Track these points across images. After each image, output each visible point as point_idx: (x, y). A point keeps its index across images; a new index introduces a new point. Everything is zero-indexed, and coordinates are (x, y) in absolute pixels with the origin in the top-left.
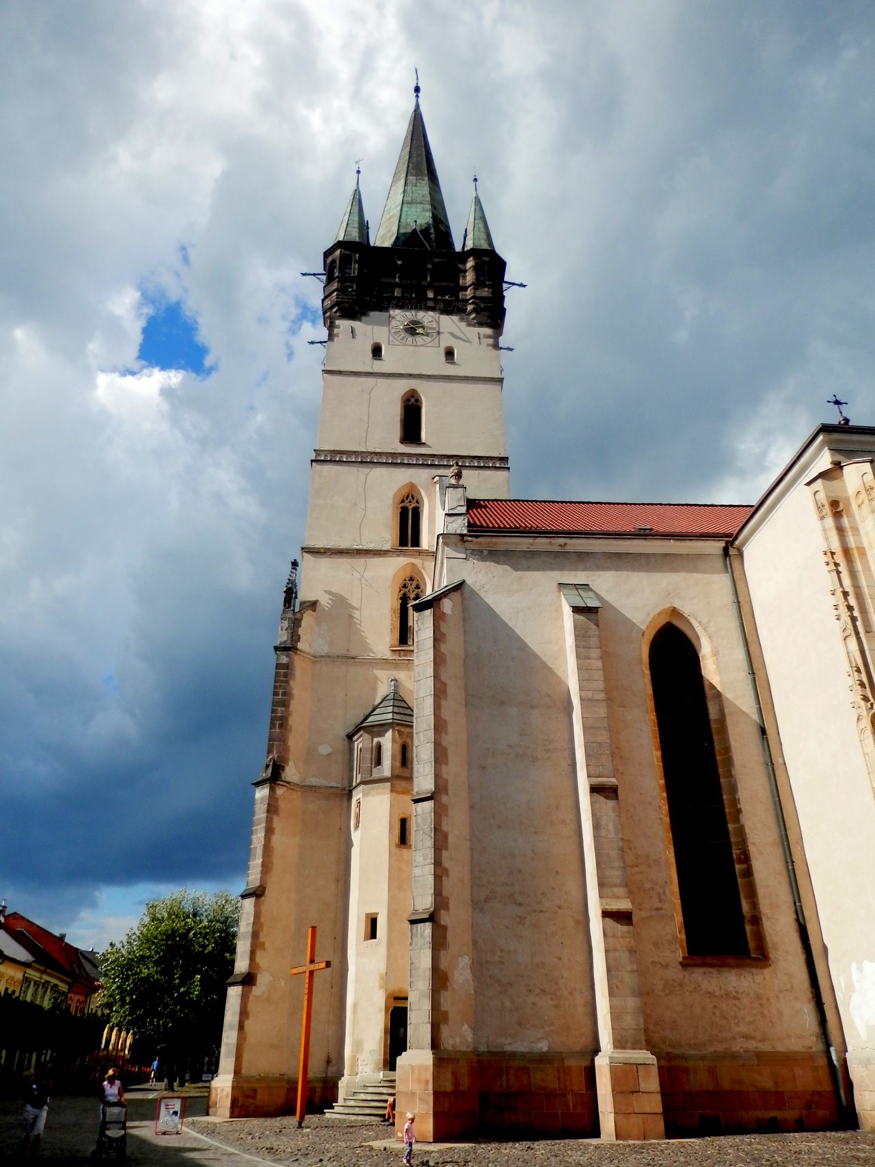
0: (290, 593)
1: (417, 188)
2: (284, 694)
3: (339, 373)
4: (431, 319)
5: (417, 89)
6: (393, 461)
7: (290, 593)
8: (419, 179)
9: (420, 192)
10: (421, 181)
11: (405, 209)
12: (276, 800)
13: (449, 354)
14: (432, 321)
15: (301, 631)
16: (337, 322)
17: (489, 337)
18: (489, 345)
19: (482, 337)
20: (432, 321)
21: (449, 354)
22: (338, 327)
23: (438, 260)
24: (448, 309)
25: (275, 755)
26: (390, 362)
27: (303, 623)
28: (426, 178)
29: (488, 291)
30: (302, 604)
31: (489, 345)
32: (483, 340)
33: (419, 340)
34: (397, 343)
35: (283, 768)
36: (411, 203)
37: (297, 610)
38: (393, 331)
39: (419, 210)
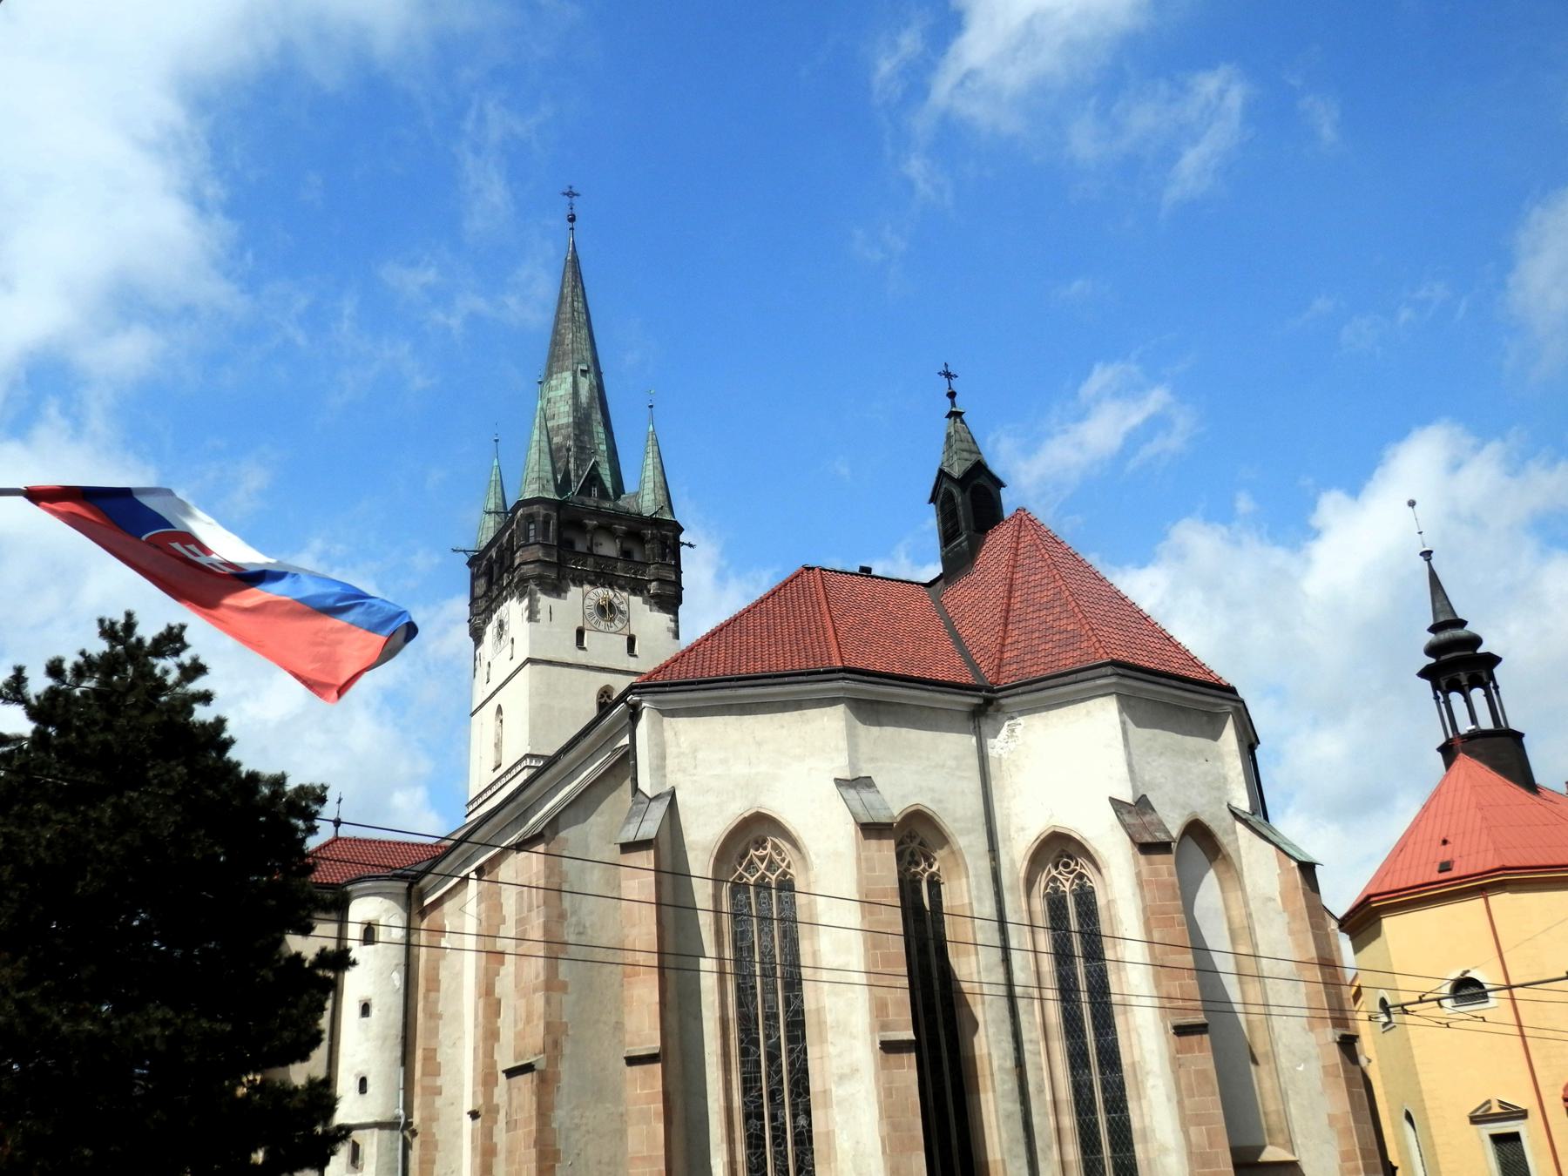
5: (572, 219)
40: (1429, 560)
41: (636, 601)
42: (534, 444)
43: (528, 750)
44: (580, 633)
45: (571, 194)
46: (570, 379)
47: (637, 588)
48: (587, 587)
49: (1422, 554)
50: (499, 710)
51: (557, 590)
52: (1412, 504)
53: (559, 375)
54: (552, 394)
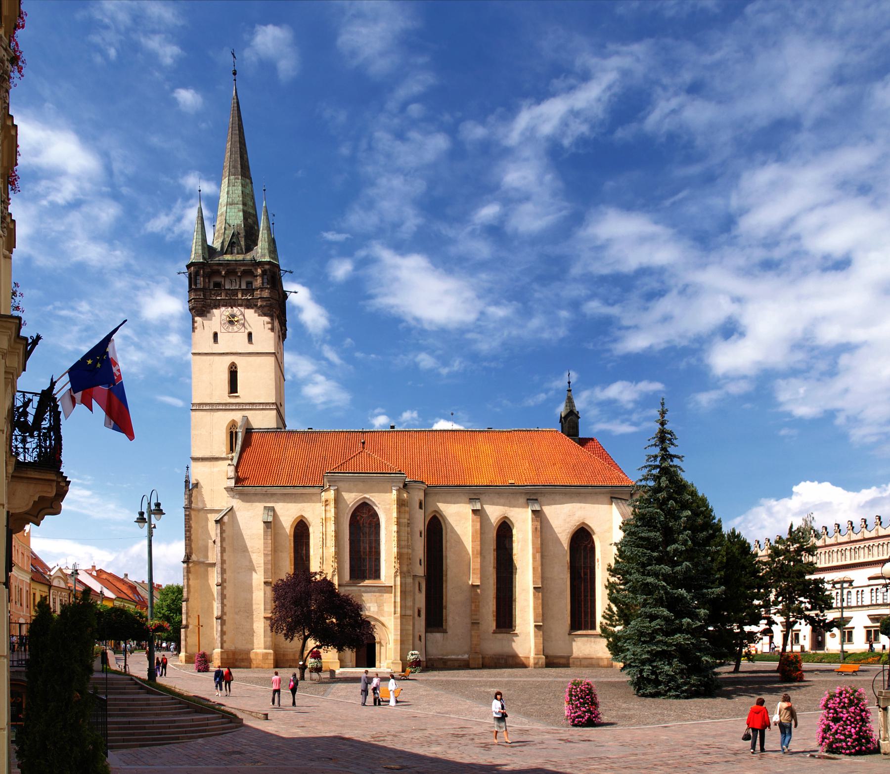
0: (187, 482)
1: (235, 188)
2: (189, 527)
3: (199, 354)
7: (187, 482)
9: (236, 192)
11: (228, 210)
17: (268, 323)
18: (269, 329)
19: (265, 323)
24: (249, 305)
28: (240, 177)
30: (193, 484)
31: (269, 329)
32: (266, 325)
33: (235, 327)
35: (191, 556)
37: (190, 488)
38: (223, 322)
39: (236, 211)
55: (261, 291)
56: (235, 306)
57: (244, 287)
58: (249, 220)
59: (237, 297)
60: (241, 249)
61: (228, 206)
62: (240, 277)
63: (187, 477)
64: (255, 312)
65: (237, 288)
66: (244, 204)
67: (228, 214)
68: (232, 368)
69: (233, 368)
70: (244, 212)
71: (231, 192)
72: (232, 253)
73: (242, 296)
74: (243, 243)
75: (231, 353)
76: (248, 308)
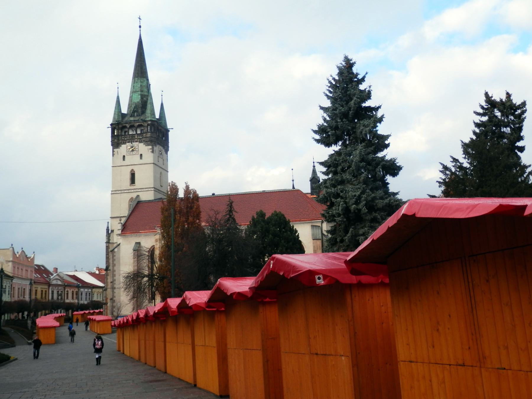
0: (108, 230)
1: (137, 84)
2: (108, 252)
4: (136, 145)
5: (140, 27)
6: (128, 191)
8: (138, 79)
9: (138, 85)
10: (138, 80)
11: (134, 95)
12: (108, 273)
13: (141, 155)
14: (136, 146)
15: (110, 238)
16: (115, 150)
17: (150, 149)
18: (151, 152)
20: (136, 146)
21: (141, 155)
22: (114, 151)
23: (138, 124)
25: (107, 265)
26: (128, 161)
27: (111, 236)
28: (140, 78)
29: (150, 134)
31: (151, 152)
34: (128, 155)
35: (109, 267)
36: (135, 92)
38: (128, 150)
39: (137, 95)
40: (293, 182)
41: (164, 150)
42: (151, 103)
43: (153, 187)
44: (158, 156)
45: (140, 19)
46: (146, 81)
47: (164, 147)
48: (159, 146)
49: (292, 180)
50: (132, 170)
51: (156, 146)
52: (292, 169)
53: (143, 78)
54: (142, 84)
55: (146, 134)
56: (134, 142)
57: (139, 132)
58: (145, 99)
59: (135, 136)
60: (139, 114)
61: (133, 93)
62: (137, 128)
63: (108, 227)
64: (144, 144)
65: (135, 133)
66: (142, 91)
67: (133, 97)
68: (132, 172)
69: (133, 172)
70: (141, 95)
71: (135, 86)
72: (134, 116)
73: (138, 137)
74: (140, 111)
75: (132, 165)
76: (140, 143)
